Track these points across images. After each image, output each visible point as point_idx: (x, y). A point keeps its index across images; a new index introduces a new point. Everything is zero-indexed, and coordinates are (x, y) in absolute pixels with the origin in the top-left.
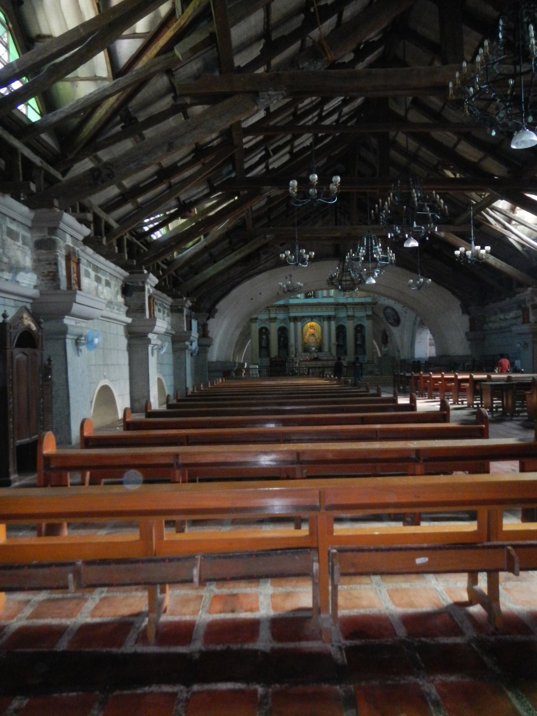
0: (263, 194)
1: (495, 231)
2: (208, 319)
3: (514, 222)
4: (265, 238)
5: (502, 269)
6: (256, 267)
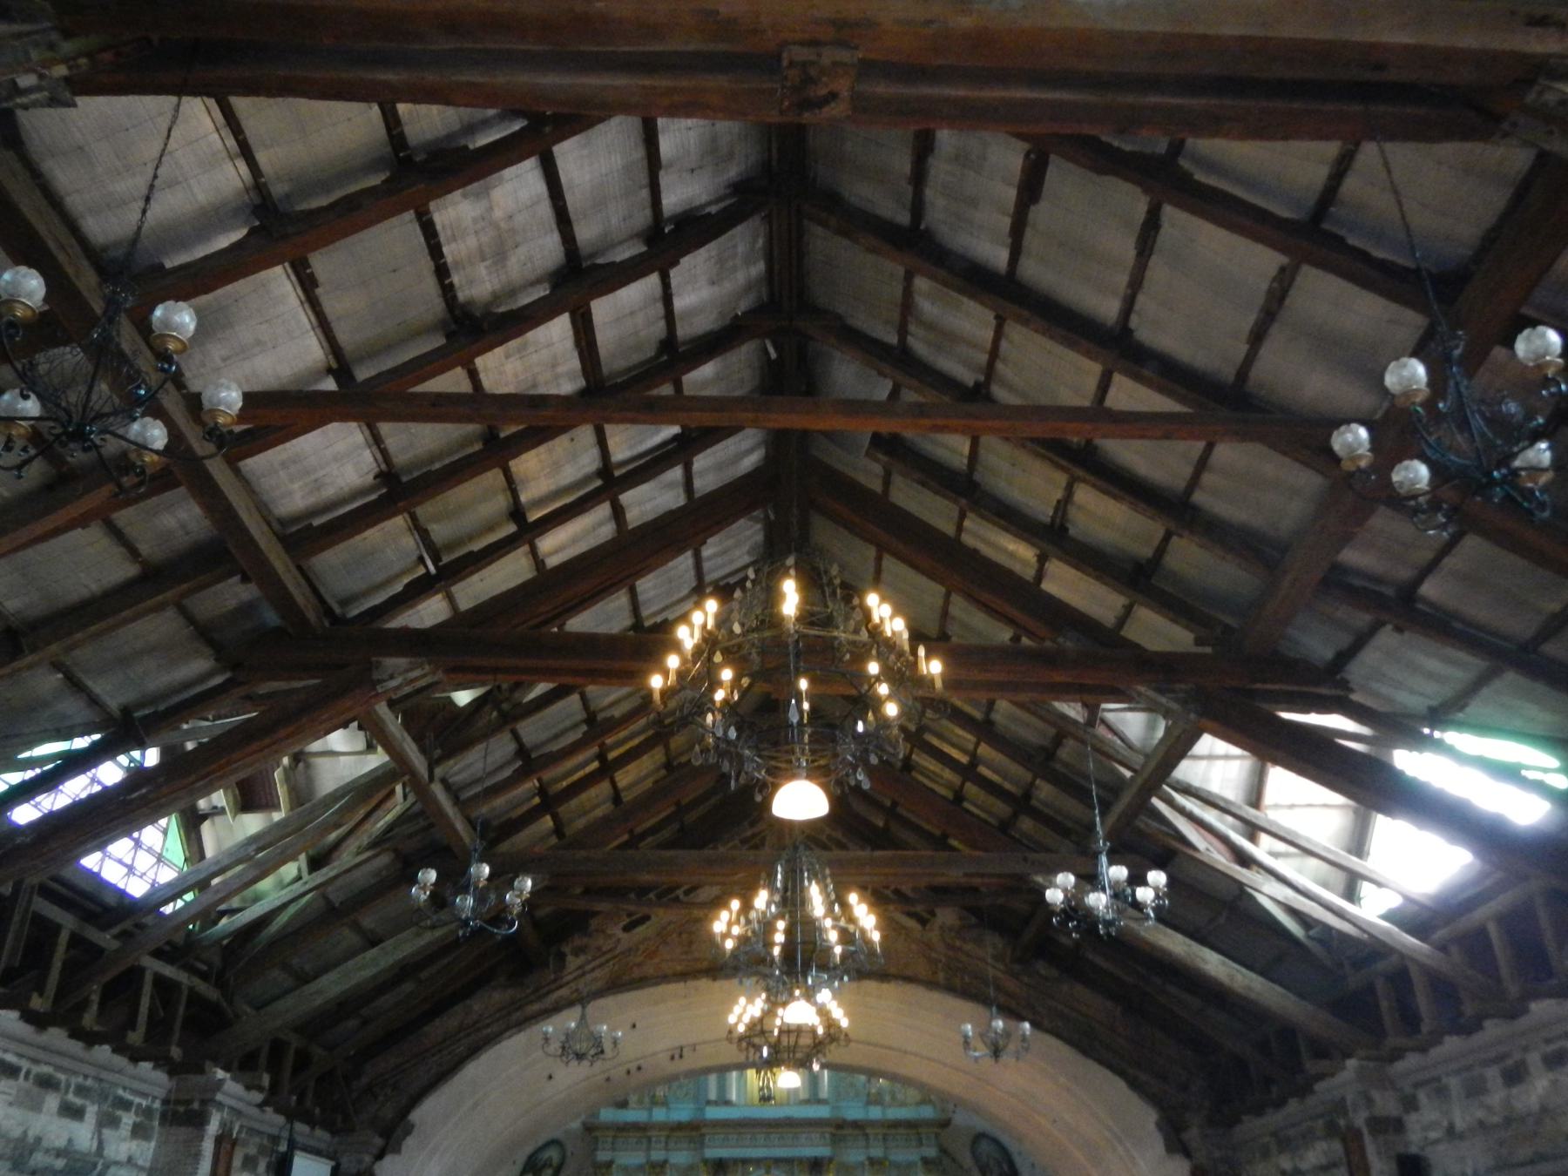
0: (380, 681)
2: (380, 1156)
5: (1253, 996)
6: (548, 993)
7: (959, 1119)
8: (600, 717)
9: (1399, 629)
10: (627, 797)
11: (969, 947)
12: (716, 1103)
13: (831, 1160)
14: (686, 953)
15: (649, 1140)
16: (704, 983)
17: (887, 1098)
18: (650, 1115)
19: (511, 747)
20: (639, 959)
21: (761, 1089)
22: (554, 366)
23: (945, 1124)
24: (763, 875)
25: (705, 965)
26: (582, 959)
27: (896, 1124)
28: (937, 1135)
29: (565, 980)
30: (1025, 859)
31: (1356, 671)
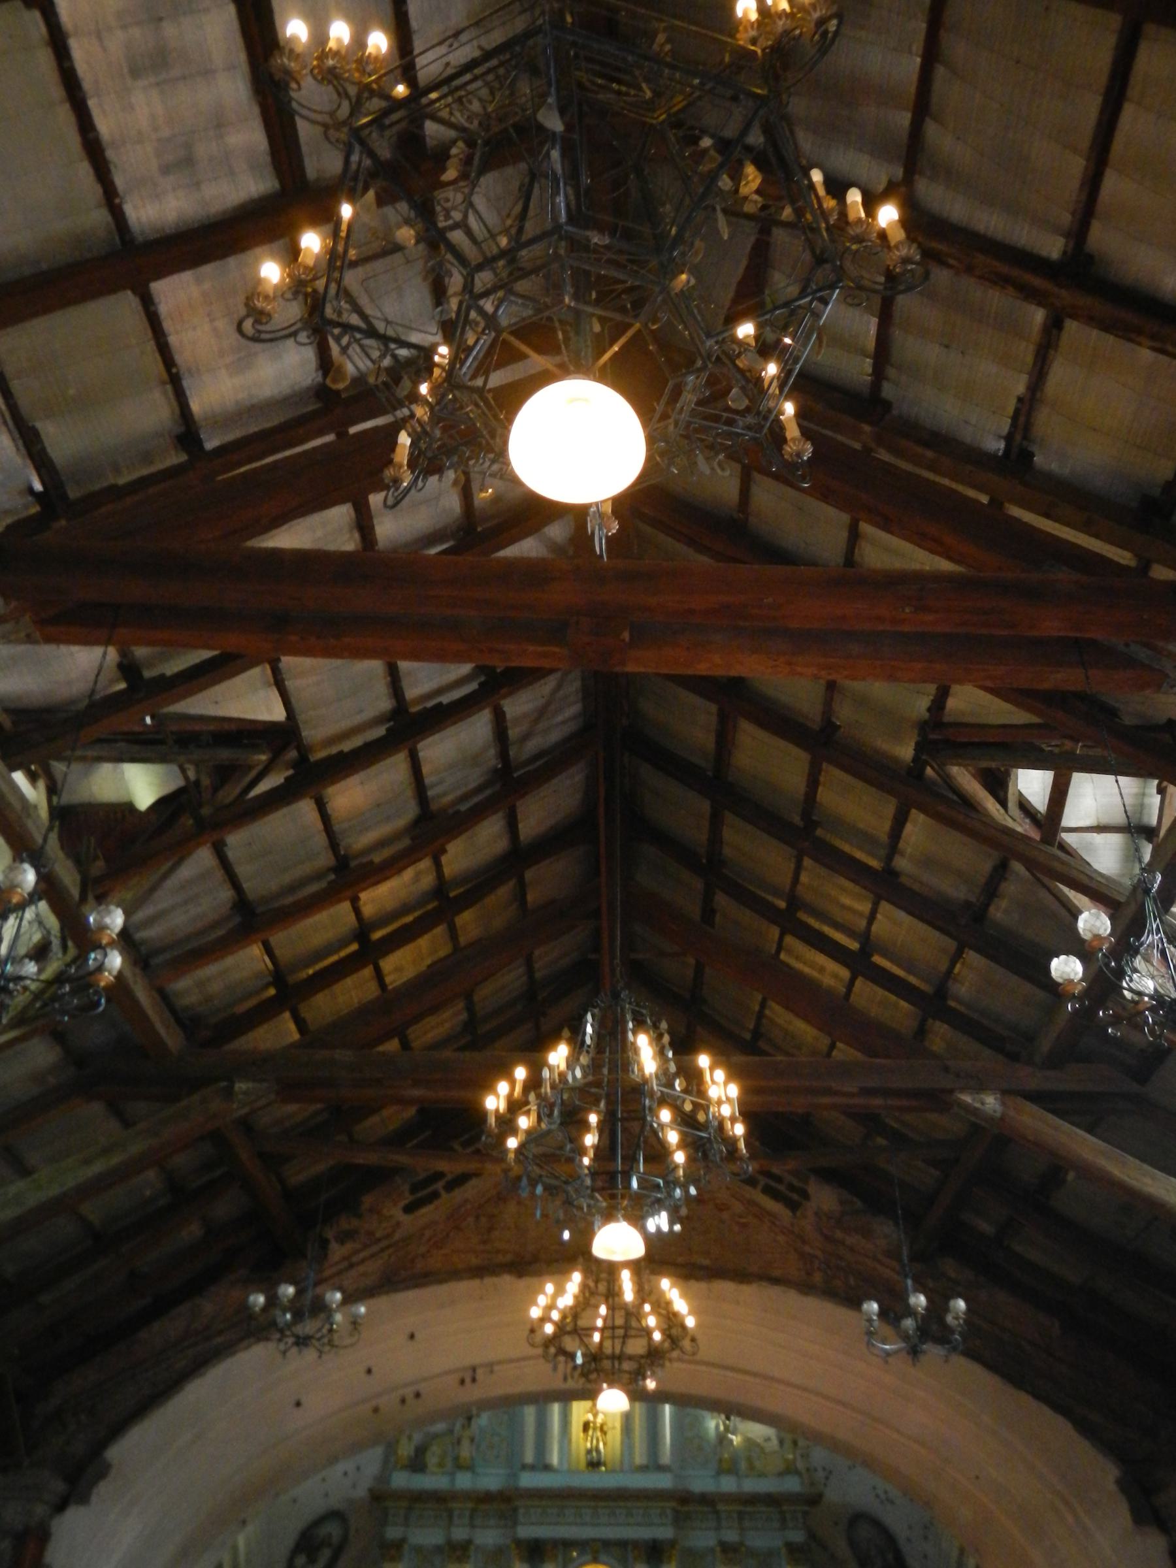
2: (61, 1507)
4: (229, 1093)
7: (832, 1495)
8: (353, 864)
12: (533, 1468)
13: (672, 1543)
14: (484, 1242)
15: (450, 1517)
16: (507, 1279)
17: (743, 1465)
18: (453, 1481)
20: (423, 1249)
21: (589, 1452)
23: (813, 1500)
24: (566, 1033)
25: (509, 1258)
26: (349, 1246)
27: (753, 1500)
28: (805, 1513)
29: (327, 1273)
30: (946, 1069)
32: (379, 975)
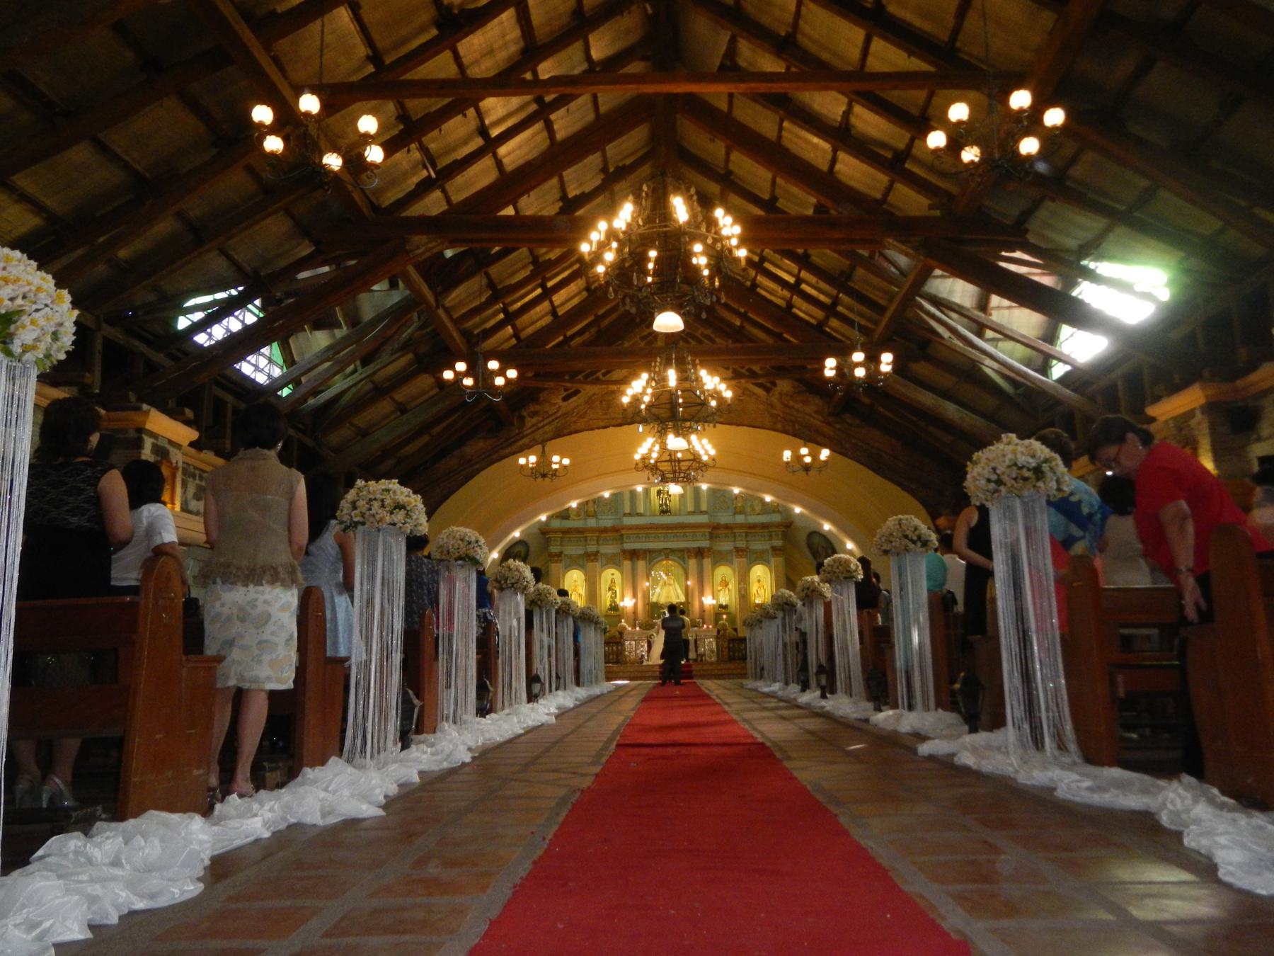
1: (952, 350)
3: (989, 334)
8: (541, 260)
9: (1053, 200)
10: (561, 312)
11: (799, 406)
12: (630, 514)
13: (709, 549)
17: (749, 509)
19: (485, 281)
22: (504, 36)
26: (535, 420)
27: (752, 526)
31: (1033, 225)
32: (551, 302)
